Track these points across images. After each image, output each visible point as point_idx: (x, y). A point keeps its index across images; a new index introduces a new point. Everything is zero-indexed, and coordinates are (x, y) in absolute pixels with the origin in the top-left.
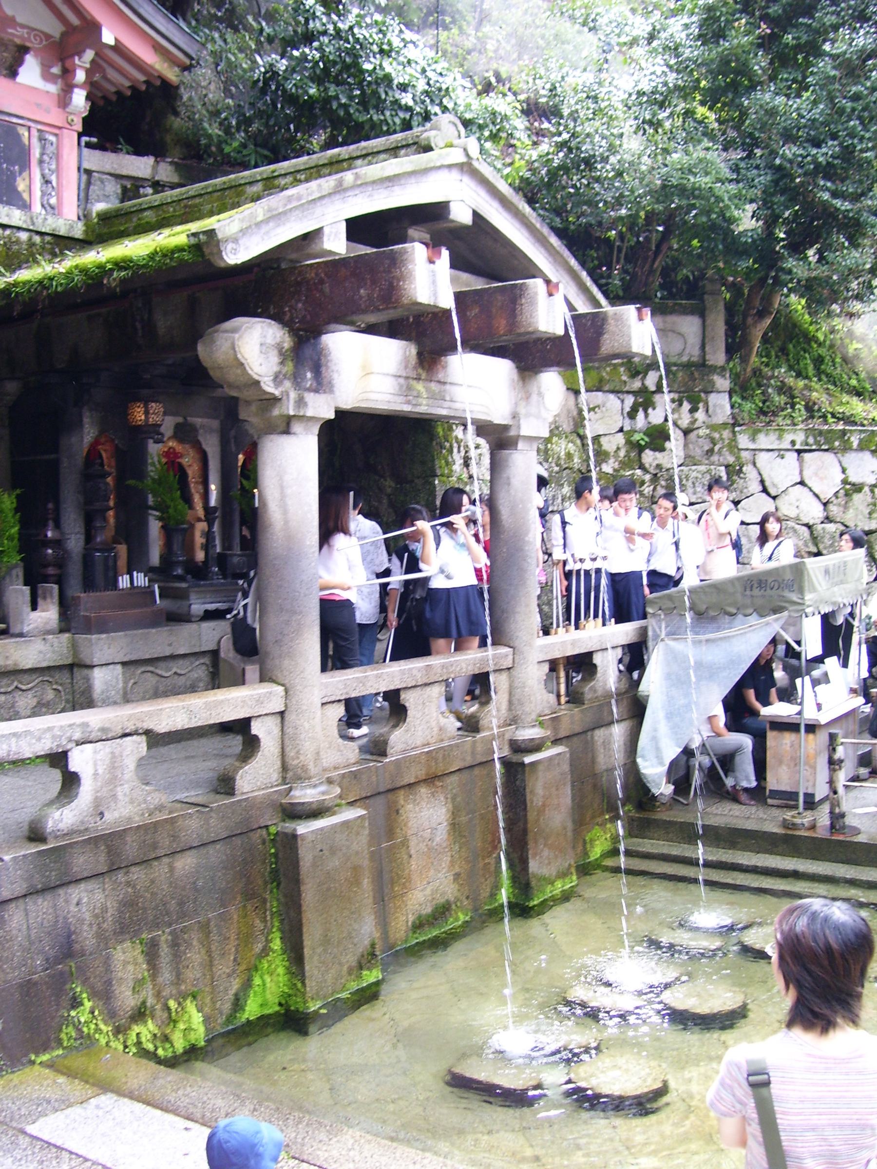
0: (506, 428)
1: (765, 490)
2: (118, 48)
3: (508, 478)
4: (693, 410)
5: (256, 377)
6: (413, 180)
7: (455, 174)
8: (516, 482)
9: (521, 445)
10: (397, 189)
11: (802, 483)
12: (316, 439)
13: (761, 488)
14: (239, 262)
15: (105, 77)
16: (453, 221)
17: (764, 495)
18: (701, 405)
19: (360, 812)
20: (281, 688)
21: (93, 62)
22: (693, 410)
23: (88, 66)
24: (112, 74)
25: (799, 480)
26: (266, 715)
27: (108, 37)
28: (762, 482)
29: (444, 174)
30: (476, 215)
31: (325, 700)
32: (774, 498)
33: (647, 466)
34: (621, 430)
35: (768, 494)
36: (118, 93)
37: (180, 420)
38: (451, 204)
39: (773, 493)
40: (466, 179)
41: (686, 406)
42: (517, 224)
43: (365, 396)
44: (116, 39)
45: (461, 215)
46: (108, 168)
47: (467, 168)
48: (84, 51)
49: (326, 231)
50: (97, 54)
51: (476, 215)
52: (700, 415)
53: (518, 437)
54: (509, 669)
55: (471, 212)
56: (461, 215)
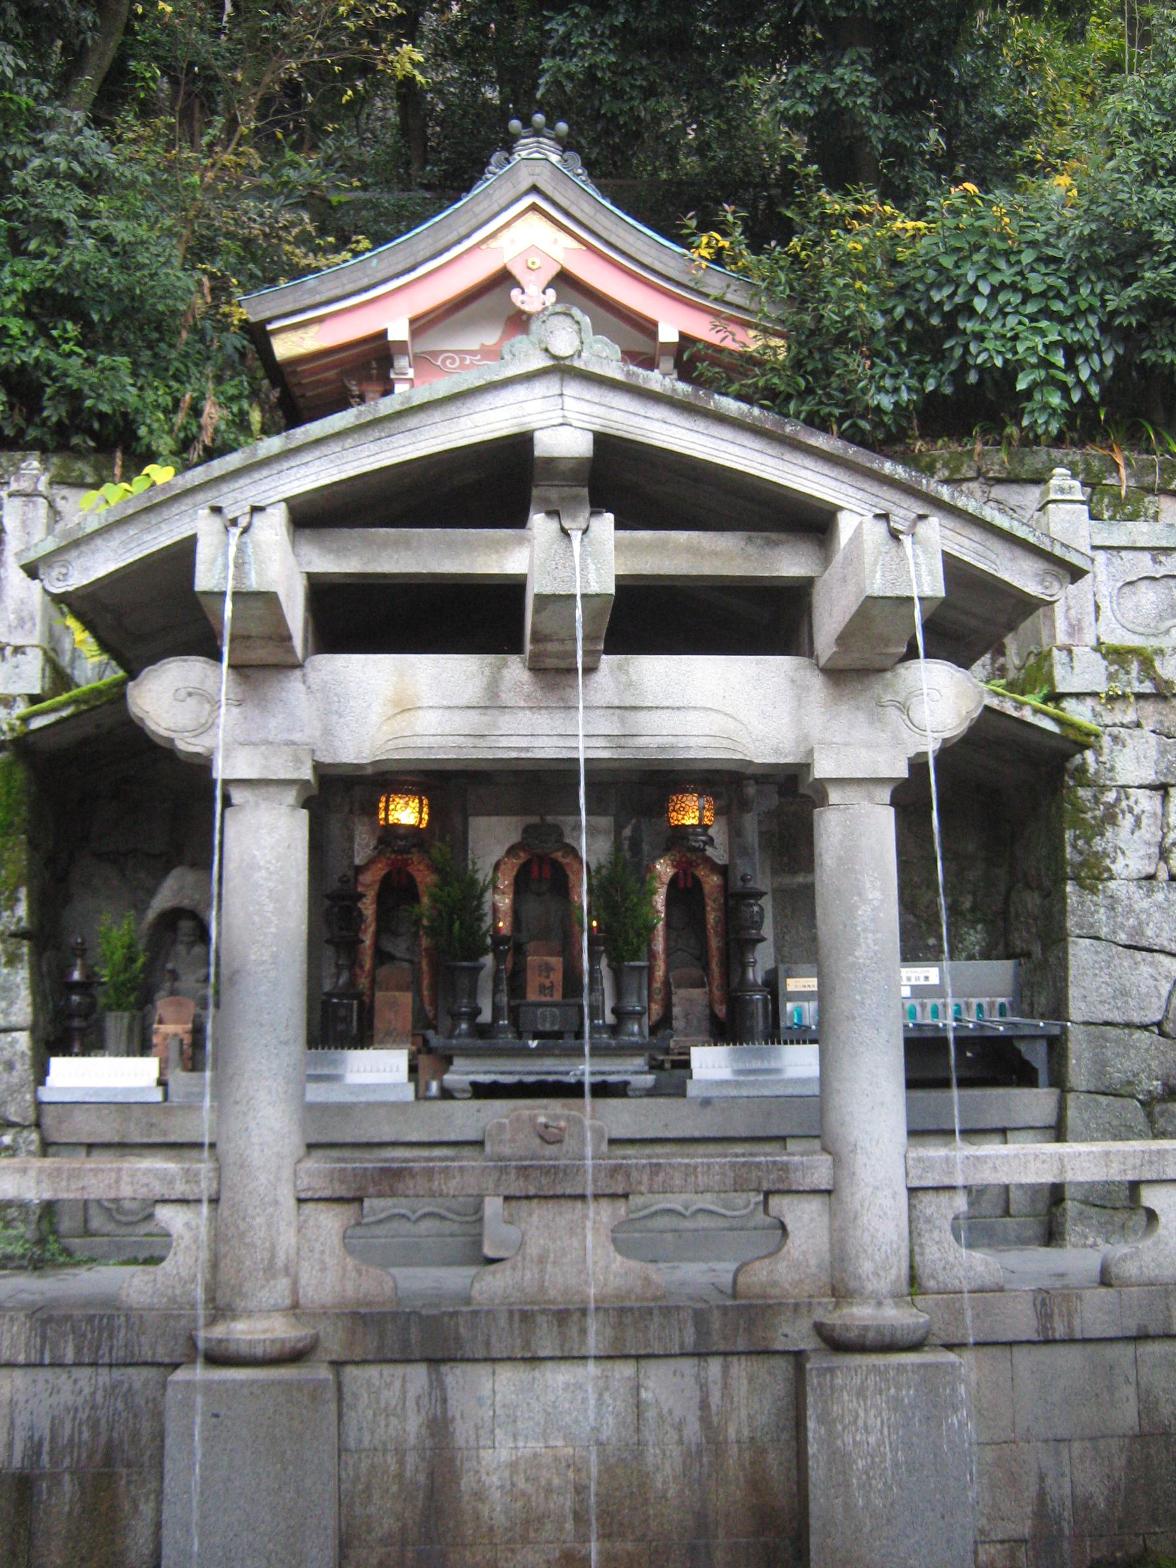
5: (166, 733)
6: (437, 415)
7: (541, 388)
9: (834, 796)
10: (400, 440)
14: (70, 589)
16: (550, 461)
29: (520, 392)
30: (602, 441)
31: (303, 1195)
37: (535, 820)
38: (538, 435)
40: (573, 389)
43: (400, 743)
53: (823, 782)
55: (590, 436)
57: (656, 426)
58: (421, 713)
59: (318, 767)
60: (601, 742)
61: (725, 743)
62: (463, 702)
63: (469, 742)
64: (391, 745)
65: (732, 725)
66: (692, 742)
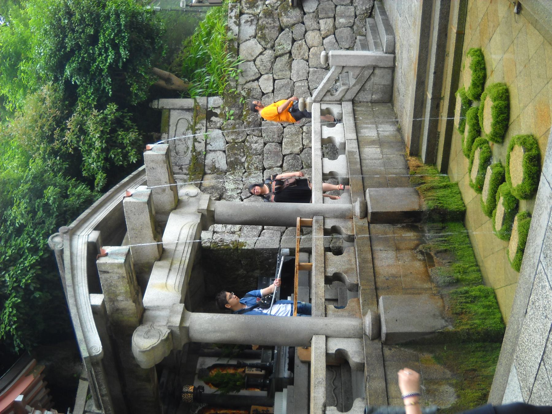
0: (203, 216)
1: (257, 79)
2: (25, 394)
3: (228, 215)
4: (216, 115)
5: (159, 341)
8: (230, 212)
11: (254, 61)
12: (193, 313)
13: (256, 82)
14: (101, 347)
15: (41, 401)
16: (97, 240)
17: (260, 80)
18: (214, 111)
19: (381, 300)
20: (314, 336)
21: (32, 406)
22: (216, 115)
23: (33, 409)
24: (39, 397)
25: (253, 62)
26: (326, 345)
27: (20, 398)
28: (253, 81)
31: (324, 315)
32: (261, 75)
33: (243, 139)
34: (224, 152)
35: (259, 78)
36: (49, 394)
38: (89, 241)
39: (259, 75)
40: (78, 233)
41: (214, 119)
42: (104, 208)
43: (176, 288)
44: (21, 394)
45: (94, 236)
46: (83, 402)
47: (72, 233)
48: (26, 410)
49: (93, 303)
50: (28, 404)
51: (96, 229)
52: (218, 111)
53: (208, 210)
54: (324, 218)
56: (94, 236)
57: (95, 220)
58: (168, 283)
59: (181, 302)
60: (186, 248)
61: (193, 226)
62: (167, 274)
63: (180, 274)
64: (177, 290)
65: (187, 225)
66: (191, 231)
